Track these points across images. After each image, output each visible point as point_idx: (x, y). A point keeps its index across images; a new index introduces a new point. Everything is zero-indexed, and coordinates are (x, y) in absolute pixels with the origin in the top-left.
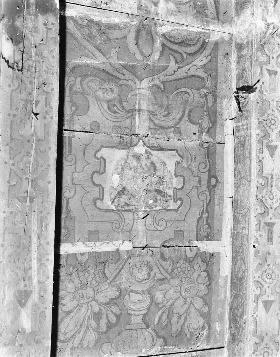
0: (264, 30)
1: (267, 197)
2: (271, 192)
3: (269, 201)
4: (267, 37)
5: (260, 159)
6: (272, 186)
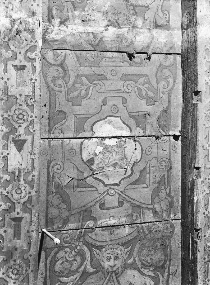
0: (9, 26)
1: (14, 192)
2: (18, 187)
3: (16, 196)
4: (12, 33)
5: (5, 154)
6: (19, 181)
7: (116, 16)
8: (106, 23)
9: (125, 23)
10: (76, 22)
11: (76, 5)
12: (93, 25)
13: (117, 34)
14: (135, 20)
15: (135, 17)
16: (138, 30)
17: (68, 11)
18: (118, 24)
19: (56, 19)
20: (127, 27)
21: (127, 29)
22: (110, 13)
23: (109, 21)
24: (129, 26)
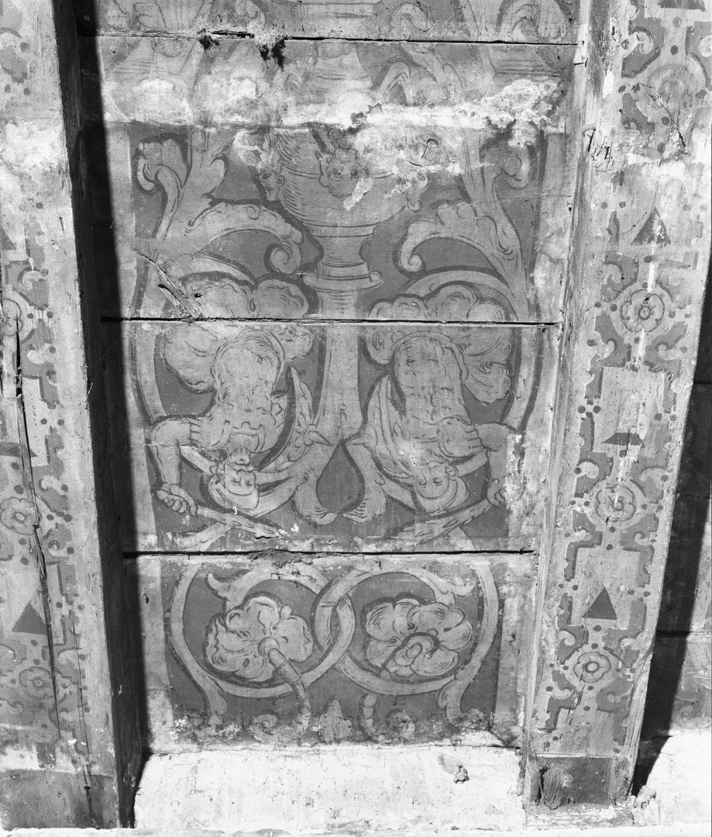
7: (324, 163)
8: (360, 141)
9: (292, 144)
10: (460, 139)
11: (455, 193)
12: (402, 132)
13: (321, 102)
14: (257, 154)
15: (259, 166)
16: (247, 121)
17: (482, 173)
18: (316, 136)
19: (522, 146)
20: (286, 127)
21: (286, 121)
22: (346, 172)
23: (348, 148)
24: (281, 131)
